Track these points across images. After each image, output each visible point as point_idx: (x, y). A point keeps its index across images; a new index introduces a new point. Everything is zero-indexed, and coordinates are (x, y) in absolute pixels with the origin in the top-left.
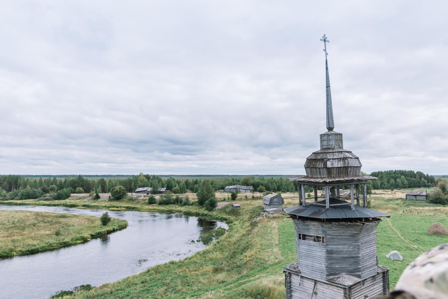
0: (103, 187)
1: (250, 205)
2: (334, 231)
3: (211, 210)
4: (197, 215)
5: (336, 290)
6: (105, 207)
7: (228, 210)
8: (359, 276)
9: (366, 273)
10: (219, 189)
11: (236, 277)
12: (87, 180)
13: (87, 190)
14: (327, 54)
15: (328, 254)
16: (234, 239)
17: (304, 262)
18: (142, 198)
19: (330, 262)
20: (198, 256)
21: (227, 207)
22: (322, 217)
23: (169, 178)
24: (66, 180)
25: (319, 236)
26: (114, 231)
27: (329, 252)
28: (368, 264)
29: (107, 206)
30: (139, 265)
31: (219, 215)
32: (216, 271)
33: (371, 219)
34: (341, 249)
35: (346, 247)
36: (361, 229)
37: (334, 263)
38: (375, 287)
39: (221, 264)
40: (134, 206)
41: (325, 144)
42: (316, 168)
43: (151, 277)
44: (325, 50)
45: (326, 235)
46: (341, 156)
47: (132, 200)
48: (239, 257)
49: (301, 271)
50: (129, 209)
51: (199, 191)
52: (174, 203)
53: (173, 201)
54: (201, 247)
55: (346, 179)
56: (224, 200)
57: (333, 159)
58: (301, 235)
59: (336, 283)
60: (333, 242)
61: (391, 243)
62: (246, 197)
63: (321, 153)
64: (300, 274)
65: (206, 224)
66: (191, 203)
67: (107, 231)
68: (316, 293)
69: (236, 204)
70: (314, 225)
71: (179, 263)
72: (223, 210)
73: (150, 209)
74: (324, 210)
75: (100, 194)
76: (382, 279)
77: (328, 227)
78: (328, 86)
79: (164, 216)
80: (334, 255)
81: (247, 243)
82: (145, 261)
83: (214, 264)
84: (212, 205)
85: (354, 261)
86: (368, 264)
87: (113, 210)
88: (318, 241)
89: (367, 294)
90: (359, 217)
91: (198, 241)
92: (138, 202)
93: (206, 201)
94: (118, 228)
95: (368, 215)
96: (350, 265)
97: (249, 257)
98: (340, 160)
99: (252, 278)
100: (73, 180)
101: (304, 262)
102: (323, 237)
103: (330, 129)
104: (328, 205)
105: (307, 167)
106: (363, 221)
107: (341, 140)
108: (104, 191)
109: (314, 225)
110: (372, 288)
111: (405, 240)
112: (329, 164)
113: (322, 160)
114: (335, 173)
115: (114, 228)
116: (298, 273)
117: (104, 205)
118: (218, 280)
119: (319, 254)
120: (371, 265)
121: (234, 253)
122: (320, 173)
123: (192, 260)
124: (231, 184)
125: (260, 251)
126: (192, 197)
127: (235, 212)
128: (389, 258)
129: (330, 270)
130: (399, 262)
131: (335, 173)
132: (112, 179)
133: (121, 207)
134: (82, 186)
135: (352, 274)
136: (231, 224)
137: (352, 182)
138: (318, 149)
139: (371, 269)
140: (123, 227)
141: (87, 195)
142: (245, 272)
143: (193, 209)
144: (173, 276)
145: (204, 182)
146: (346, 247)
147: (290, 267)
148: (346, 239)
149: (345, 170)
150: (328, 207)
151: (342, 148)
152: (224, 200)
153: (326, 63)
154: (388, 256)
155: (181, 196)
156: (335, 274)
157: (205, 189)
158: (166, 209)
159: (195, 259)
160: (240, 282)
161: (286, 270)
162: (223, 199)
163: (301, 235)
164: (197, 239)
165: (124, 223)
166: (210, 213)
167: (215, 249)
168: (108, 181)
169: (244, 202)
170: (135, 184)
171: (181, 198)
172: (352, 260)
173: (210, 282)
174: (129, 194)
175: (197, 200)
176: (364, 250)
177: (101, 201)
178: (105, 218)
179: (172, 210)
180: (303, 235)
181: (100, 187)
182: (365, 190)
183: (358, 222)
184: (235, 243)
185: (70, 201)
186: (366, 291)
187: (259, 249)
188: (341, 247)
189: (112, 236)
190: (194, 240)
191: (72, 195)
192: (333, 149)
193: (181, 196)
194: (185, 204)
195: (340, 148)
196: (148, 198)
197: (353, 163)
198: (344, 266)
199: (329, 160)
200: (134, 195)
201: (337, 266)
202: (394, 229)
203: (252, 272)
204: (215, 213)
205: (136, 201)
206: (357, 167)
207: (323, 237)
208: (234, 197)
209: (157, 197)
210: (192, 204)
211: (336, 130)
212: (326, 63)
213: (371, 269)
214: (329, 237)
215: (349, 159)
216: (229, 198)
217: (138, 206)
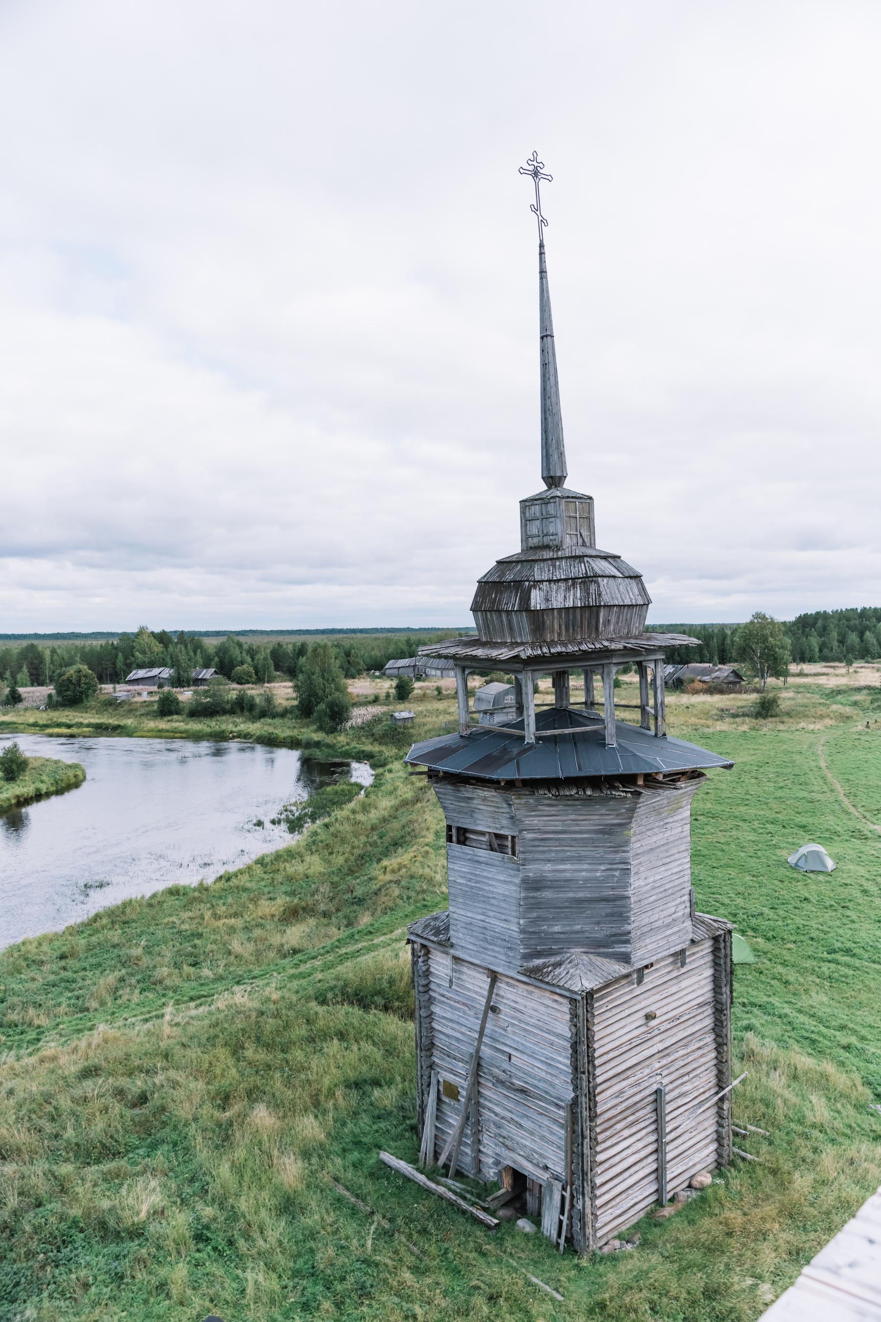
0: (36, 668)
1: (445, 712)
2: (541, 818)
3: (332, 731)
4: (293, 744)
5: (549, 1003)
6: (35, 725)
7: (378, 729)
8: (625, 958)
9: (650, 947)
10: (369, 670)
11: (336, 933)
14: (543, 222)
15: (526, 889)
16: (374, 816)
17: (462, 912)
18: (145, 697)
19: (535, 915)
20: (258, 870)
21: (377, 720)
22: (503, 774)
23: (223, 639)
25: (502, 832)
26: (39, 797)
27: (533, 885)
28: (658, 916)
29: (41, 722)
30: (82, 898)
31: (354, 744)
32: (292, 915)
33: (660, 778)
35: (586, 867)
36: (633, 810)
37: (546, 919)
38: (684, 984)
39: (313, 895)
40: (116, 723)
41: (535, 531)
42: (499, 611)
43: (94, 939)
45: (521, 831)
46: (579, 570)
47: (112, 704)
48: (375, 870)
49: (453, 940)
50: (102, 730)
51: (301, 677)
52: (232, 712)
53: (228, 707)
54: (282, 839)
55: (584, 647)
56: (376, 700)
57: (550, 581)
58: (454, 831)
59: (548, 983)
61: (810, 820)
62: (439, 689)
63: (517, 562)
64: (452, 951)
65: (321, 770)
66: (280, 710)
67: (18, 797)
68: (494, 1009)
69: (403, 712)
70: (484, 799)
71: (194, 890)
72: (367, 730)
73: (160, 731)
74: (515, 751)
75: (21, 690)
76: (710, 958)
77: (527, 804)
78: (546, 336)
79: (205, 747)
80: (548, 894)
81: (404, 827)
82: (101, 886)
83: (293, 894)
84: (337, 715)
85: (608, 911)
86: (656, 917)
87: (59, 736)
88: (502, 849)
89: (652, 1008)
90: (621, 771)
91: (273, 822)
92: (130, 711)
93: (321, 708)
94: (53, 789)
95: (651, 765)
96: (598, 923)
97: (393, 871)
98: (573, 585)
99: (382, 938)
101: (462, 912)
102: (513, 837)
103: (553, 480)
104: (530, 733)
105: (476, 608)
106: (640, 782)
107: (589, 519)
108: (37, 680)
109: (484, 799)
110: (674, 989)
111: (852, 809)
112: (537, 600)
113: (517, 584)
114: (556, 627)
115: (38, 790)
116: (446, 945)
117: (31, 720)
118: (282, 945)
119: (501, 889)
120: (670, 919)
121: (362, 857)
122: (511, 629)
123: (234, 882)
124: (402, 655)
125: (427, 852)
126: (283, 692)
127: (396, 734)
128: (795, 867)
129: (533, 942)
130: (821, 878)
131: (556, 627)
133: (80, 725)
135: (602, 950)
136: (381, 770)
137: (608, 657)
138: (512, 546)
139: (669, 932)
140: (67, 783)
142: (365, 920)
143: (283, 729)
144: (159, 934)
145: (315, 650)
146: (586, 867)
147: (426, 926)
148: (584, 842)
149: (591, 612)
150: (533, 741)
151: (592, 545)
152: (376, 700)
153: (541, 254)
154: (792, 859)
155: (254, 692)
156: (551, 953)
157: (317, 670)
158: (208, 730)
159: (244, 880)
160: (344, 951)
161: (413, 938)
162: (371, 698)
163: (454, 831)
164: (274, 816)
166: (329, 739)
167: (312, 846)
168: (48, 653)
169: (429, 707)
170: (126, 658)
171: (252, 697)
172: (604, 909)
173: (258, 954)
174: (108, 688)
175: (296, 703)
176: (643, 875)
177: (26, 709)
178: (12, 761)
179: (223, 732)
180: (458, 829)
181: (25, 669)
183: (616, 788)
184: (373, 828)
186: (652, 1000)
187: (427, 848)
188: (568, 867)
189: (34, 811)
190: (262, 818)
192: (558, 548)
193: (254, 692)
194: (263, 714)
195: (584, 544)
196: (156, 698)
197: (614, 592)
198: (578, 927)
199: (537, 583)
200: (121, 691)
201: (557, 929)
202: (829, 775)
203: (386, 919)
204: (342, 739)
205: (126, 707)
206: (632, 605)
207: (513, 837)
208: (403, 692)
209: (186, 695)
210: (283, 714)
212: (541, 254)
213: (669, 932)
215: (603, 582)
216: (388, 696)
217: (129, 722)
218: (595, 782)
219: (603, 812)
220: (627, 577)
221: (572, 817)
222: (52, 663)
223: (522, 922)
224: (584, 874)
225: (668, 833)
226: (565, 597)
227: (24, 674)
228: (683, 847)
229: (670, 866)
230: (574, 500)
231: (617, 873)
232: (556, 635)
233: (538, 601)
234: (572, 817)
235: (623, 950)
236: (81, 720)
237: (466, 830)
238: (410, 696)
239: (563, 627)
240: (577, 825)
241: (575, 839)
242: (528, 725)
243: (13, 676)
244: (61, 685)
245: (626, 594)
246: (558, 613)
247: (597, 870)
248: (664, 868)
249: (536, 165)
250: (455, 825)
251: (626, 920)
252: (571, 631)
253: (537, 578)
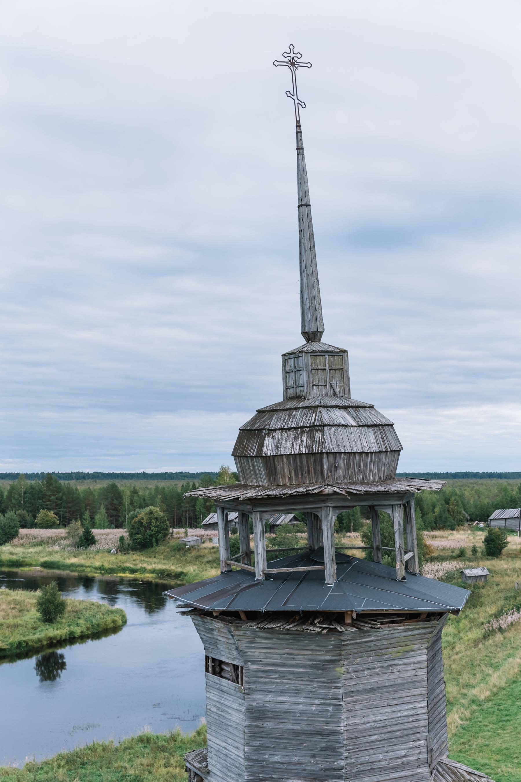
0: (116, 509)
10: (472, 520)
12: (69, 488)
13: (64, 522)
15: (250, 718)
19: (257, 743)
24: (13, 488)
27: (256, 714)
29: (107, 566)
34: (286, 706)
35: (302, 700)
37: (268, 748)
40: (179, 570)
44: (292, 94)
45: (246, 662)
47: (182, 550)
57: (282, 429)
60: (265, 683)
67: (50, 639)
75: (95, 532)
80: (268, 724)
85: (323, 745)
92: (198, 557)
96: (314, 756)
98: (302, 433)
100: (32, 487)
103: (312, 335)
105: (239, 454)
114: (287, 472)
115: (72, 633)
120: (399, 762)
131: (287, 472)
132: (139, 484)
134: (56, 506)
137: (324, 501)
138: (275, 396)
141: (62, 532)
146: (302, 700)
148: (301, 676)
151: (347, 394)
153: (299, 133)
165: (109, 619)
168: (128, 493)
172: (320, 742)
174: (178, 532)
181: (103, 510)
182: (396, 527)
185: (12, 549)
188: (286, 699)
191: (23, 531)
192: (305, 399)
200: (191, 535)
201: (277, 759)
205: (194, 553)
208: (494, 547)
211: (329, 339)
212: (299, 133)
214: (254, 667)
216: (474, 550)
218: (307, 617)
219: (313, 647)
220: (363, 426)
221: (287, 651)
222: (132, 503)
223: (246, 749)
224: (300, 707)
225: (396, 675)
226: (293, 444)
227: (101, 515)
228: (418, 691)
229: (398, 708)
230: (322, 354)
231: (330, 709)
232: (287, 480)
233: (270, 448)
234: (287, 651)
236: (145, 565)
237: (221, 662)
238: (504, 551)
239: (293, 472)
240: (294, 659)
241: (293, 673)
242: (258, 562)
243: (92, 518)
244: (133, 527)
245: (368, 442)
246: (287, 459)
247: (312, 704)
248: (389, 709)
250: (211, 655)
252: (300, 476)
253: (272, 426)
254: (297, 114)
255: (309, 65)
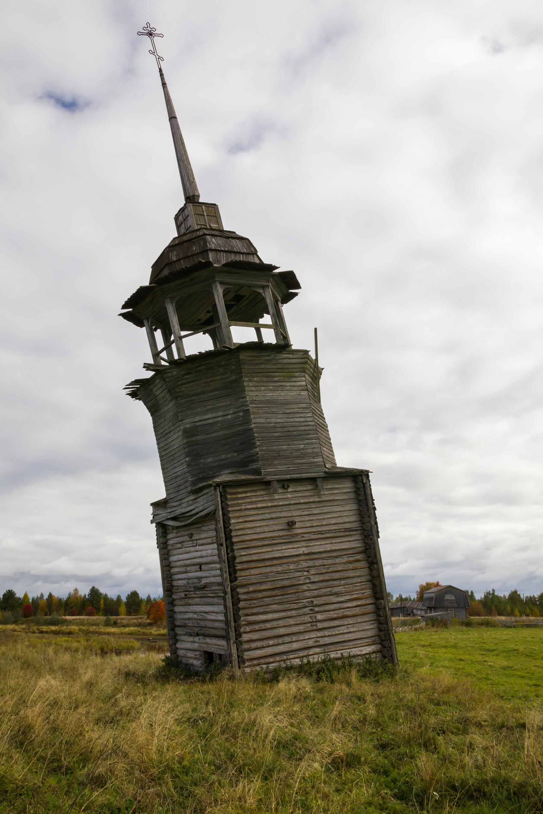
38: (325, 510)
44: (153, 52)
153: (162, 75)
188: (209, 416)
212: (162, 75)
229: (291, 416)
231: (241, 414)
235: (255, 466)
249: (150, 29)
251: (253, 445)
254: (159, 64)
255: (161, 36)
